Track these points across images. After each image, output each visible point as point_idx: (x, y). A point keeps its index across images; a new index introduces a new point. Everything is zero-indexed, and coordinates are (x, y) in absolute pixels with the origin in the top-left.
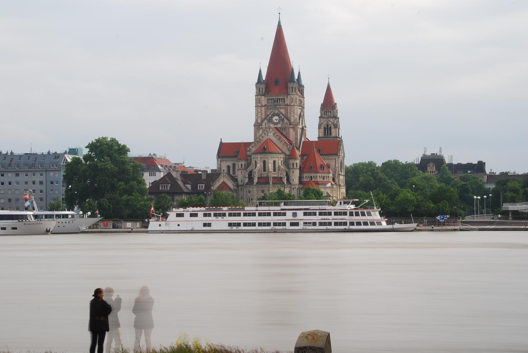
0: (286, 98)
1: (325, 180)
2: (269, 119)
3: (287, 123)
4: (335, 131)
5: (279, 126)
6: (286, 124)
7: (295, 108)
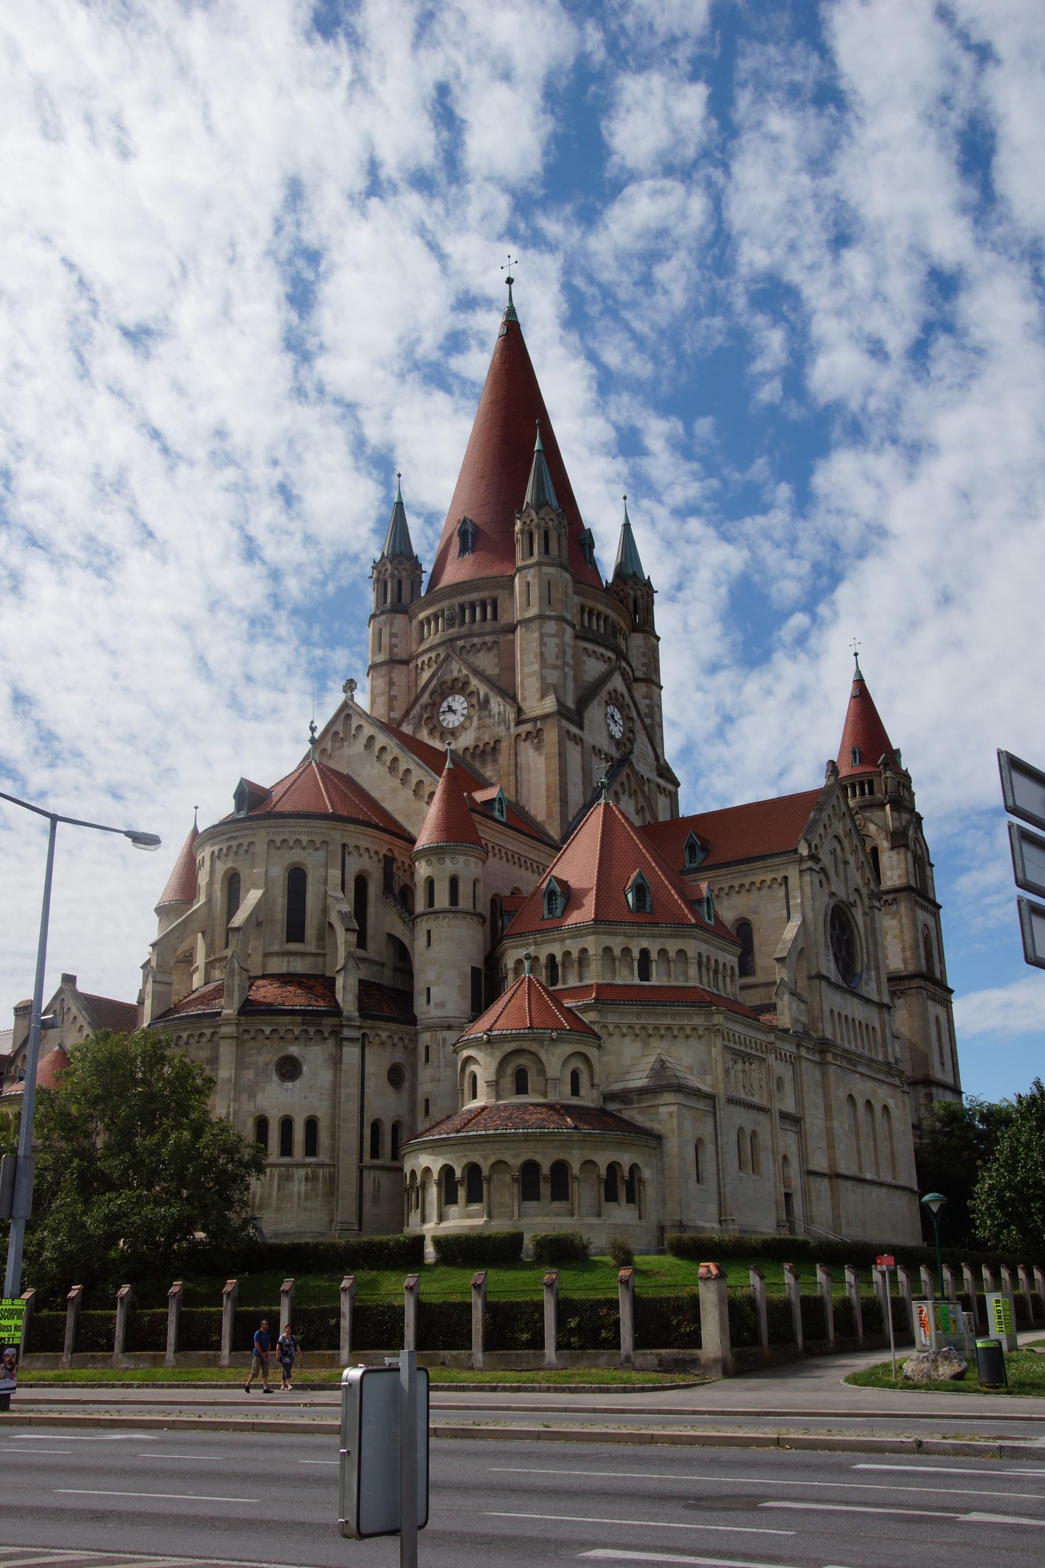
0: (501, 594)
1: (654, 981)
2: (421, 717)
3: (503, 720)
4: (895, 863)
5: (466, 740)
6: (499, 724)
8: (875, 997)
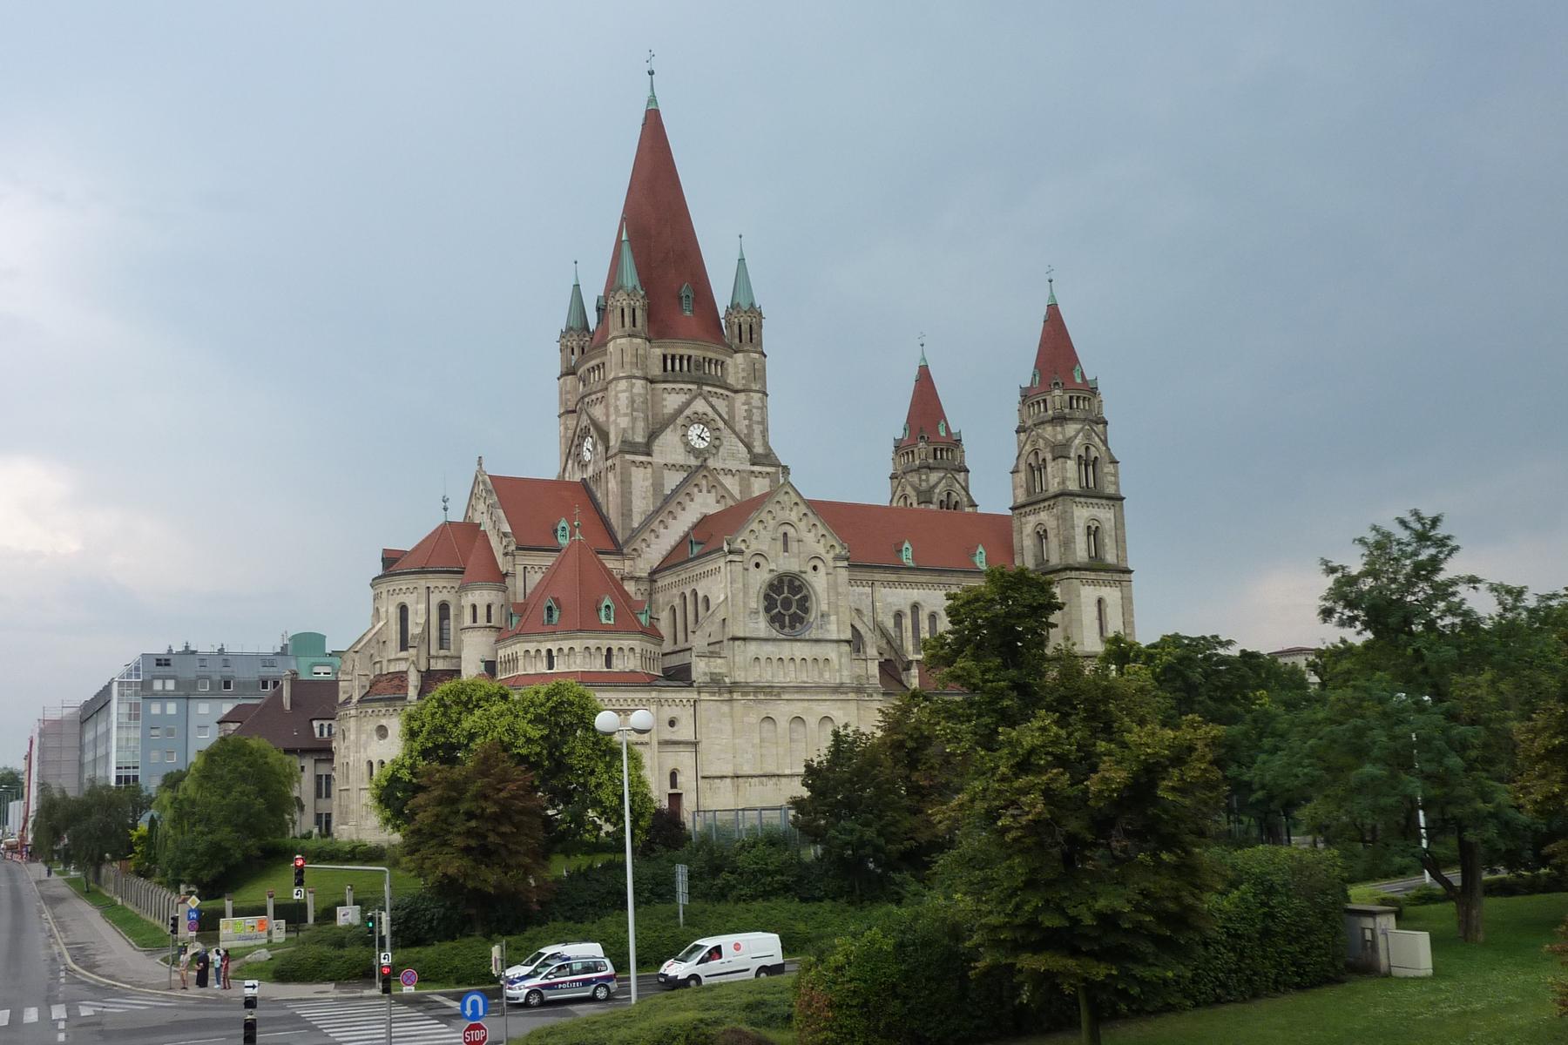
7: (618, 389)
8: (835, 637)
